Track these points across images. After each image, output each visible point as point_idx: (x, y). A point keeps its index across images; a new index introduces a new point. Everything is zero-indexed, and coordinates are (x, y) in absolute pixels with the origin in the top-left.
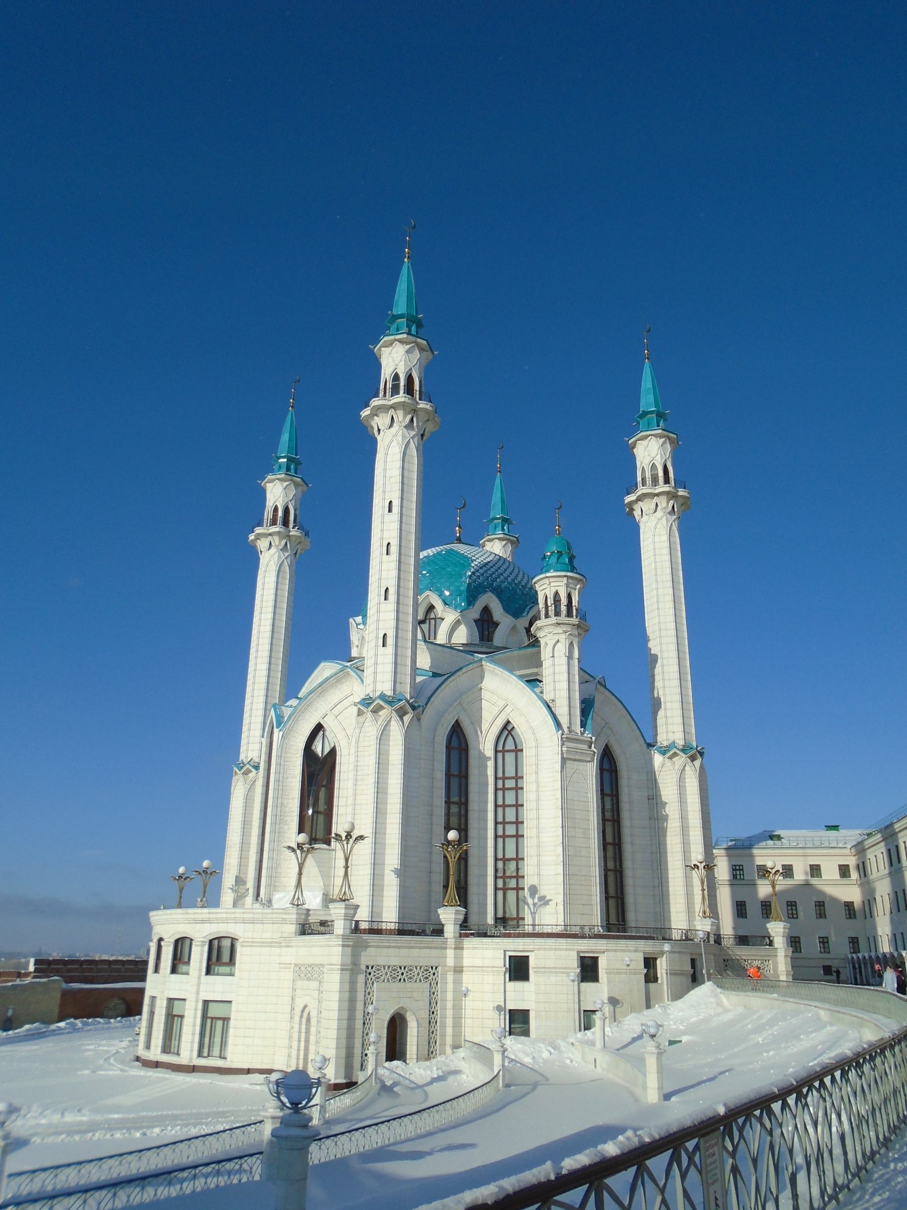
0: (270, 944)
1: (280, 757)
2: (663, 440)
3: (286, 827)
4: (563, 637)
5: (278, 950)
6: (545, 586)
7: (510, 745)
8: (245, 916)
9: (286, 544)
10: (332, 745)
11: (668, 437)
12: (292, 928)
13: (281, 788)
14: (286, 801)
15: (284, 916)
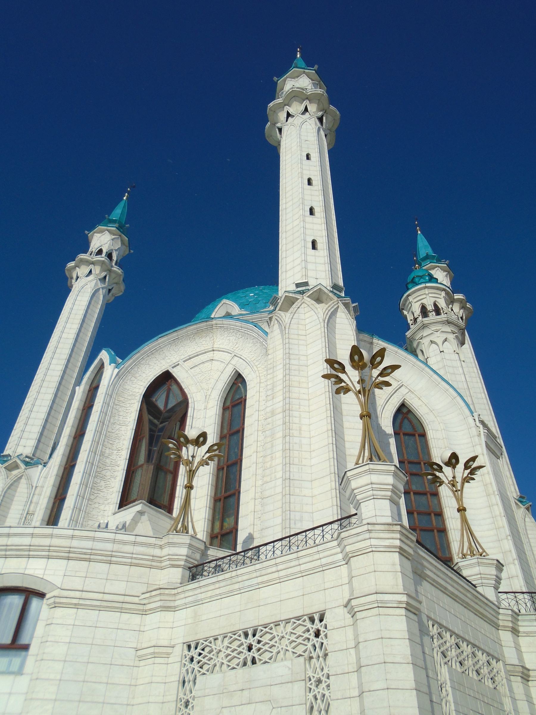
0: (119, 606)
1: (109, 395)
2: (445, 273)
3: (102, 483)
4: (451, 337)
5: (137, 619)
6: (424, 296)
7: (406, 427)
8: (75, 543)
9: (105, 277)
10: (180, 398)
11: (449, 272)
12: (176, 575)
13: (104, 432)
14: (107, 451)
15: (157, 552)
